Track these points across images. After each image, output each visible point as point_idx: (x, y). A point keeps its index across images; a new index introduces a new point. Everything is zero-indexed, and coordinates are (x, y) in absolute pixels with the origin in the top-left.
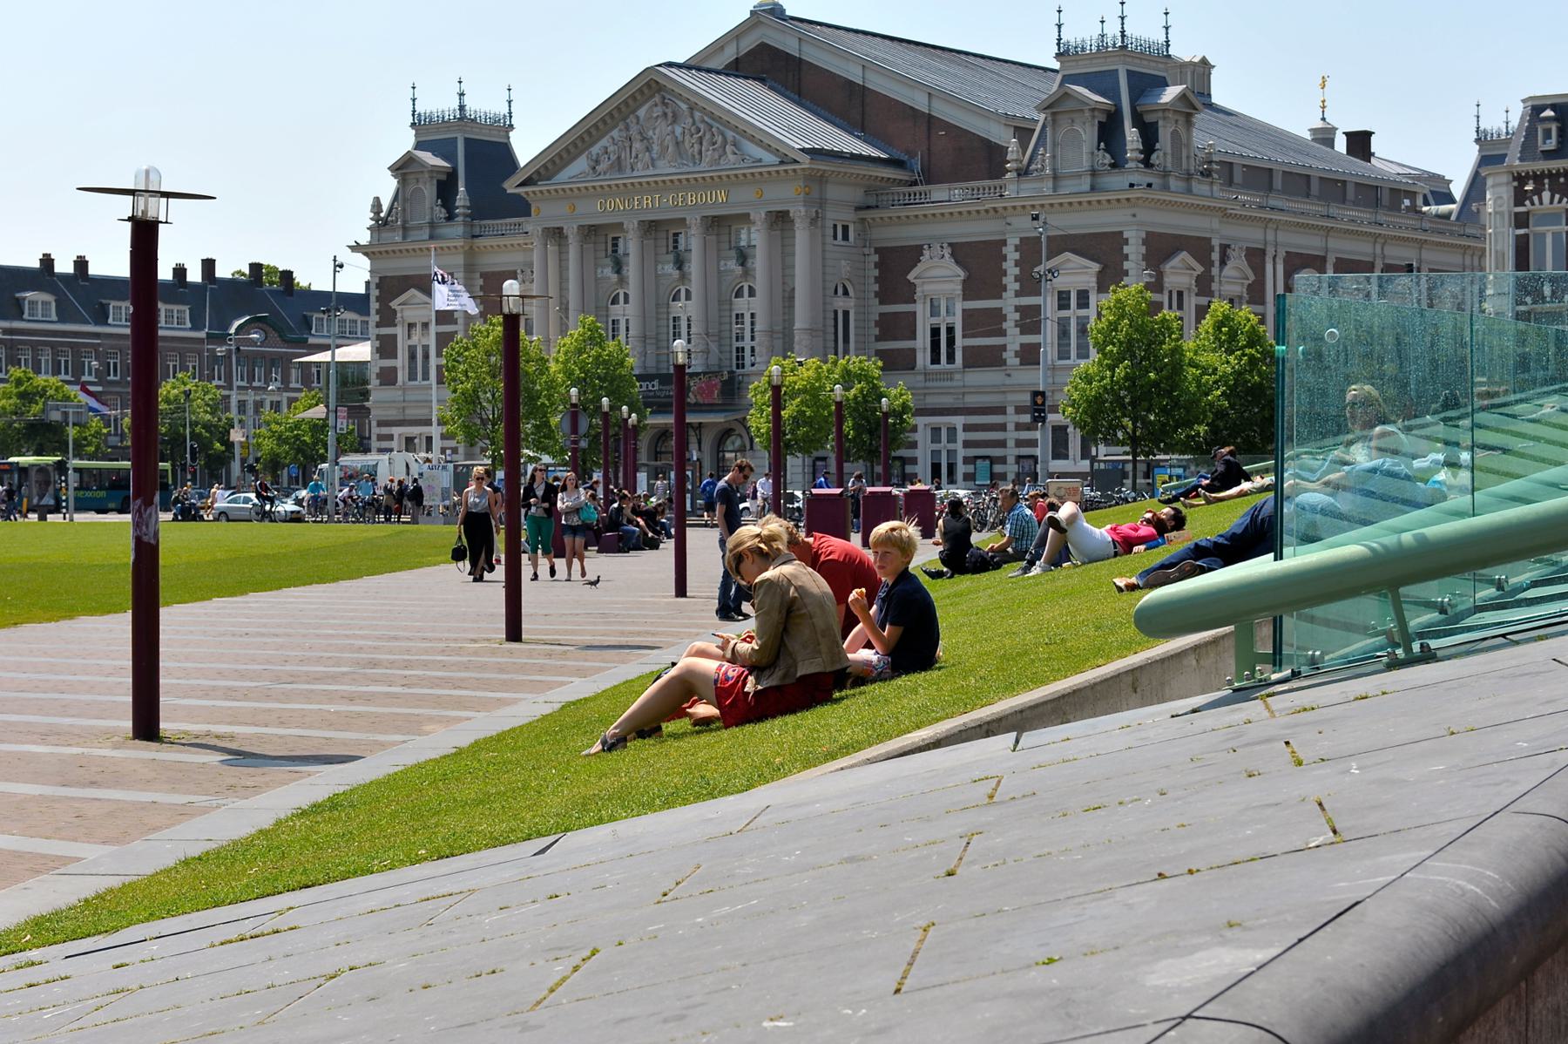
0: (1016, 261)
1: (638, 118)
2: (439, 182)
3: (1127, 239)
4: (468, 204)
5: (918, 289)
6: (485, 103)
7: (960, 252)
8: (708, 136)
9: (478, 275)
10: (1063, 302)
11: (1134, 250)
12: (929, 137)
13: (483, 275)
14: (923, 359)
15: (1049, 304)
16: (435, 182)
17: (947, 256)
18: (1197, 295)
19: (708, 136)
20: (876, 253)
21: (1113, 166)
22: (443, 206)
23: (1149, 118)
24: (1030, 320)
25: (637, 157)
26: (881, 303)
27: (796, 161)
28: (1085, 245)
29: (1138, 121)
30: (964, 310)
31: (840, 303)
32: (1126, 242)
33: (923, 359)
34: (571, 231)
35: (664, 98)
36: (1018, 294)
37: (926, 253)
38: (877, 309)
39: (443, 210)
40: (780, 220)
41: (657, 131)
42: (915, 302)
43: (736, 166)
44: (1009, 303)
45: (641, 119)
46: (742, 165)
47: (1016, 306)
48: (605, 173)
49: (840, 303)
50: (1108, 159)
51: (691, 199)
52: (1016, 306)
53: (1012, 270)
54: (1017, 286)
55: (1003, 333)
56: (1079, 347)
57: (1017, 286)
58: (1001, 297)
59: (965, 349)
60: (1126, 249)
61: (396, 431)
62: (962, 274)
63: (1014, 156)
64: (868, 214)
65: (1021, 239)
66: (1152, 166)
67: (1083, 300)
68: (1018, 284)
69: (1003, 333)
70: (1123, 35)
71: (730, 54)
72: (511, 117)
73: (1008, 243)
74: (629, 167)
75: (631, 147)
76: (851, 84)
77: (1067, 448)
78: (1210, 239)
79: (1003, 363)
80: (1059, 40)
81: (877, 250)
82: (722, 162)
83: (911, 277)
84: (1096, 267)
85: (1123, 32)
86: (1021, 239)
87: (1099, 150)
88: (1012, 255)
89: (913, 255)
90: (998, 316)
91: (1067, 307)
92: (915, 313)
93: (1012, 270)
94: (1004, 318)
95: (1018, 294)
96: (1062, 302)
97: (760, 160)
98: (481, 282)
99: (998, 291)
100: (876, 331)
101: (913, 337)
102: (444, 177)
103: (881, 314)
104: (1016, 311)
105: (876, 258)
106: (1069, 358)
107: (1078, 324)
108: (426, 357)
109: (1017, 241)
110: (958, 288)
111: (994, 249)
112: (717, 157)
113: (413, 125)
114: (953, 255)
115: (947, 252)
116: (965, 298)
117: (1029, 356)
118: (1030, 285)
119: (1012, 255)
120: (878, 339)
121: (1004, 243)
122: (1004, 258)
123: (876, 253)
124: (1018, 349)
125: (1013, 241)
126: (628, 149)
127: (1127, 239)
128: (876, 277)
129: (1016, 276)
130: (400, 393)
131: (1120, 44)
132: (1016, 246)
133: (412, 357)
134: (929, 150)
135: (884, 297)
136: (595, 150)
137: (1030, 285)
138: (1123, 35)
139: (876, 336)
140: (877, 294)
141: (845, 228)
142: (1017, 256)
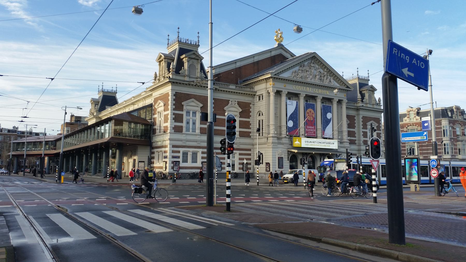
19: (326, 76)
40: (340, 102)
43: (334, 85)
51: (320, 91)
55: (355, 137)
61: (182, 150)
65: (363, 116)
86: (363, 116)
95: (363, 128)
104: (362, 132)
118: (365, 127)
121: (355, 116)
125: (361, 116)
130: (185, 135)
133: (188, 123)
137: (365, 127)
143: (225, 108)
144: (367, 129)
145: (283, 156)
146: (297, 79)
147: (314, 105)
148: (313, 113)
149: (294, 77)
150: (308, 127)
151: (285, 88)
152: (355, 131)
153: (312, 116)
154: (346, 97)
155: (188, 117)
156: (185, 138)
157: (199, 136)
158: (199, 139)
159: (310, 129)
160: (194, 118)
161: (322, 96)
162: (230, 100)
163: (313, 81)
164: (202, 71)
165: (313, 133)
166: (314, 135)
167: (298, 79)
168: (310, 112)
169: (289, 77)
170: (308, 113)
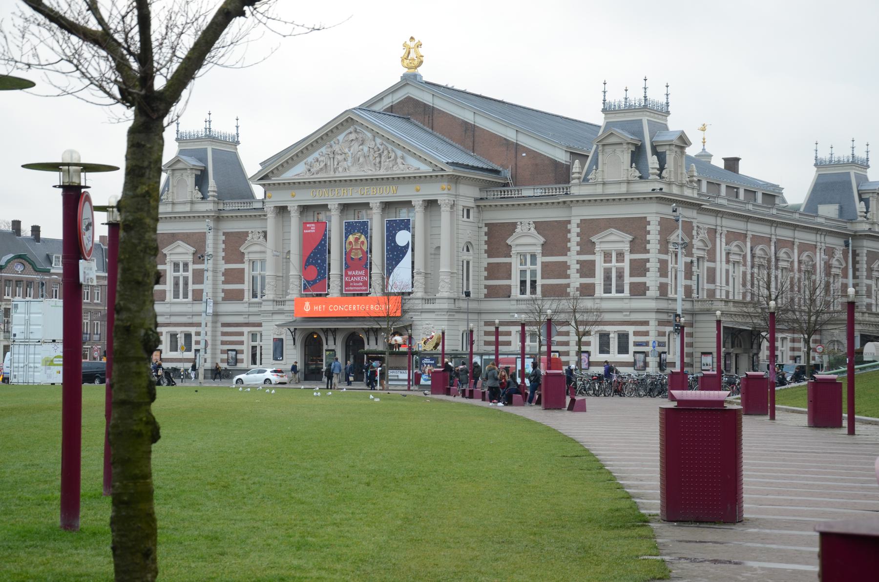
0: (578, 233)
1: (338, 140)
2: (197, 176)
3: (649, 222)
4: (216, 190)
5: (512, 249)
6: (223, 127)
7: (540, 227)
8: (386, 153)
9: (222, 234)
10: (607, 257)
11: (654, 229)
12: (516, 157)
13: (224, 234)
14: (516, 292)
15: (599, 259)
16: (194, 176)
17: (532, 229)
18: (685, 256)
19: (386, 153)
20: (486, 226)
21: (641, 177)
22: (200, 190)
23: (660, 150)
24: (587, 269)
25: (338, 164)
26: (489, 257)
27: (442, 170)
28: (622, 224)
29: (655, 152)
30: (542, 262)
31: (466, 256)
32: (649, 223)
33: (516, 292)
34: (293, 207)
35: (356, 129)
36: (579, 253)
37: (519, 227)
38: (486, 261)
39: (200, 193)
41: (352, 149)
42: (511, 256)
43: (404, 172)
44: (573, 259)
45: (341, 141)
46: (408, 171)
47: (577, 261)
48: (317, 173)
49: (466, 256)
50: (637, 174)
52: (577, 261)
53: (574, 238)
54: (578, 248)
55: (568, 277)
56: (617, 286)
57: (578, 248)
58: (566, 255)
59: (543, 286)
60: (648, 228)
62: (542, 240)
63: (577, 170)
64: (482, 203)
66: (663, 178)
67: (620, 256)
68: (579, 247)
69: (568, 277)
70: (646, 100)
71: (387, 102)
72: (238, 136)
73: (572, 222)
74: (332, 170)
75: (334, 158)
76: (466, 123)
77: (609, 347)
78: (691, 222)
79: (568, 294)
80: (604, 100)
81: (486, 225)
82: (394, 169)
83: (509, 242)
84: (630, 238)
85: (645, 97)
87: (632, 167)
88: (574, 229)
89: (511, 227)
90: (565, 266)
91: (610, 261)
92: (511, 263)
93: (574, 238)
94: (569, 267)
95: (579, 253)
96: (606, 259)
97: (419, 169)
98: (223, 238)
99: (565, 251)
100: (486, 274)
101: (509, 277)
102: (199, 173)
103: (488, 264)
105: (486, 229)
106: (611, 293)
107: (617, 272)
108: (186, 284)
109: (579, 222)
110: (538, 250)
111: (563, 227)
112: (391, 166)
113: (177, 140)
114: (535, 228)
115: (532, 226)
116: (543, 255)
117: (587, 291)
118: (587, 246)
119: (574, 229)
120: (486, 278)
121: (569, 222)
122: (569, 231)
123: (486, 226)
124: (578, 286)
125: (575, 221)
126: (332, 159)
127: (649, 222)
128: (486, 241)
129: (577, 242)
130: (168, 306)
131: (643, 104)
132: (578, 224)
133: (176, 284)
134: (516, 164)
135: (490, 253)
136: (310, 159)
138: (646, 100)
139: (485, 277)
140: (486, 252)
141: (468, 211)
142: (578, 230)
143: (242, 249)
144: (595, 254)
145: (283, 337)
146: (311, 177)
147: (365, 224)
148: (363, 243)
150: (350, 273)
151: (293, 199)
152: (566, 262)
153: (361, 249)
154: (446, 192)
155: (177, 274)
156: (168, 310)
157: (190, 305)
158: (190, 310)
159: (356, 276)
160: (185, 274)
162: (247, 232)
163: (355, 172)
164: (197, 187)
165: (361, 284)
166: (364, 288)
168: (357, 240)
170: (350, 243)
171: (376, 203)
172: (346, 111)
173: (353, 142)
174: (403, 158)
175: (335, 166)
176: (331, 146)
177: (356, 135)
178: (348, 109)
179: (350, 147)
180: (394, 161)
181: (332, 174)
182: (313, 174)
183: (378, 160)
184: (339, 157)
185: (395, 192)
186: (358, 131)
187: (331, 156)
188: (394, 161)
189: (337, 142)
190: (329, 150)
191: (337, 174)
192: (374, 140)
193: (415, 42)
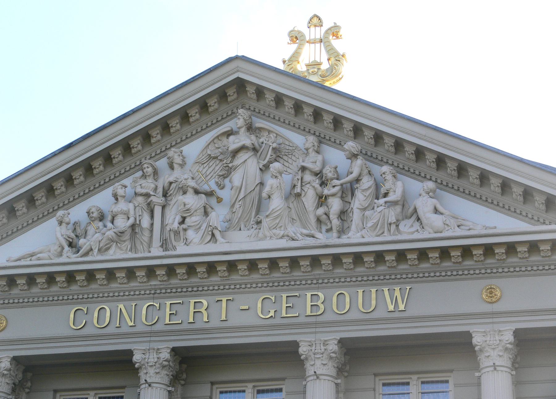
19: (367, 182)
45: (190, 161)
46: (459, 232)
75: (164, 207)
82: (401, 227)
112: (393, 219)
149: (60, 254)
161: (339, 336)
167: (95, 256)
169: (19, 260)
171: (325, 343)
172: (237, 58)
173: (242, 157)
174: (431, 194)
175: (176, 225)
176: (156, 173)
177: (253, 137)
178: (233, 55)
179: (228, 172)
180: (398, 208)
181: (156, 251)
182: (86, 254)
183: (335, 205)
184: (191, 200)
185: (402, 307)
186: (258, 125)
187: (158, 199)
188: (398, 208)
189: (178, 160)
190: (148, 185)
191: (181, 249)
192: (318, 152)
193: (324, 29)
